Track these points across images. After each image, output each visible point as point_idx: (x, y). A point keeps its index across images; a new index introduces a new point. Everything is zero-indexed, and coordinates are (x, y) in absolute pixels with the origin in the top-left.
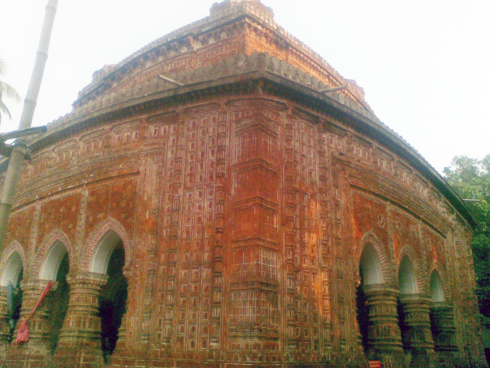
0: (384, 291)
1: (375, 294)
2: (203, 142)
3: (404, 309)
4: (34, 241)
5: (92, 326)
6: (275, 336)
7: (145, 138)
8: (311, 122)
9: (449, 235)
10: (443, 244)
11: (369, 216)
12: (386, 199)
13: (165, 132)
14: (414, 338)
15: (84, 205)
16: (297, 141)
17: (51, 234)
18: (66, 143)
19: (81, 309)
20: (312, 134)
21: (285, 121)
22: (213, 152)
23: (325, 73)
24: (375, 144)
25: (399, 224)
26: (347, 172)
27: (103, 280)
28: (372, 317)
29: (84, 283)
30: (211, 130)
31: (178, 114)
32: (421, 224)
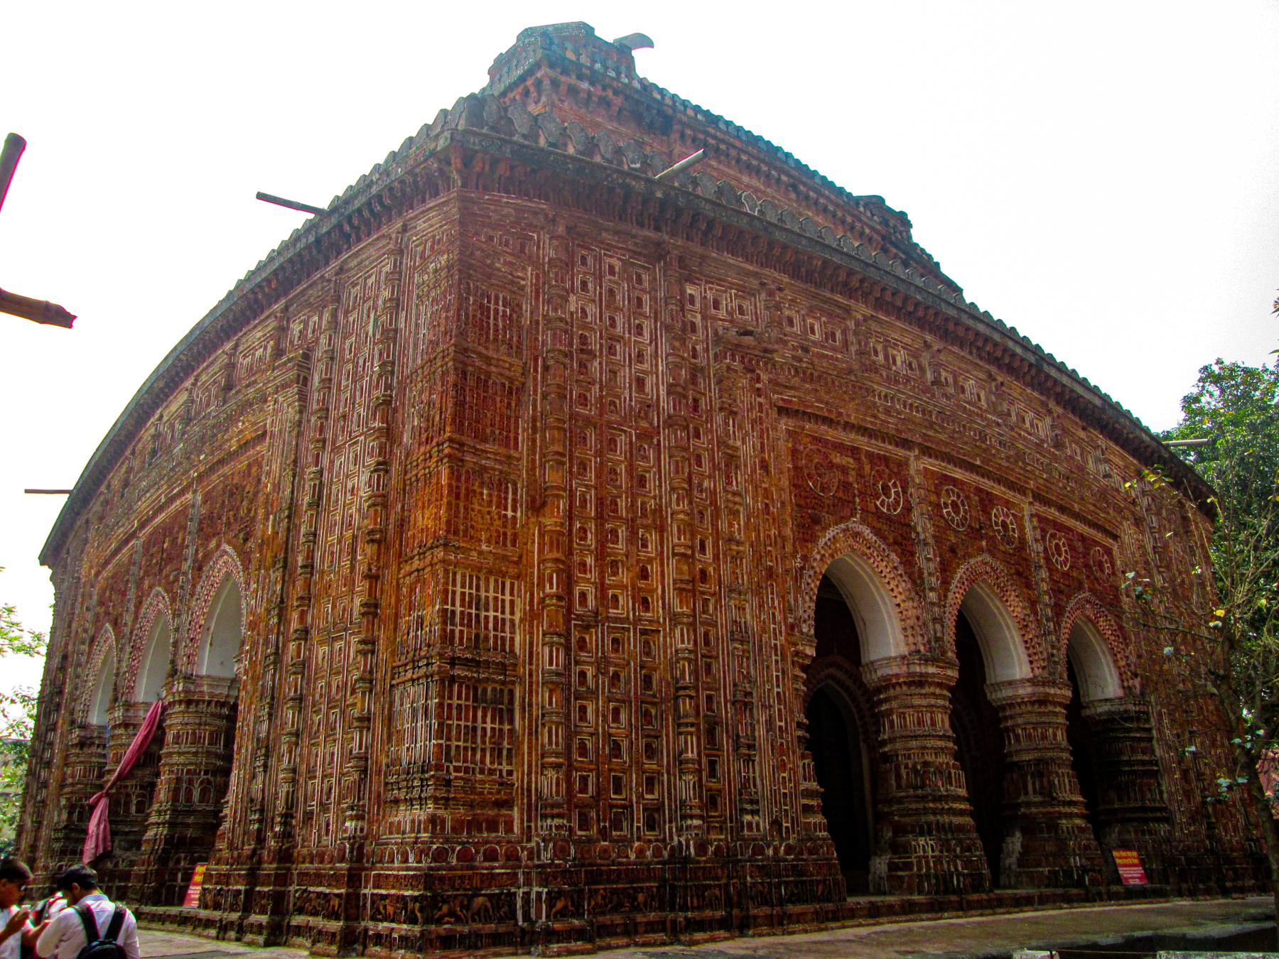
0: (909, 674)
1: (888, 683)
3: (999, 721)
6: (502, 796)
9: (1128, 532)
10: (1109, 552)
11: (846, 486)
12: (906, 444)
14: (1026, 793)
19: (182, 759)
23: (784, 178)
24: (862, 310)
25: (954, 505)
26: (764, 377)
28: (884, 743)
32: (1031, 503)
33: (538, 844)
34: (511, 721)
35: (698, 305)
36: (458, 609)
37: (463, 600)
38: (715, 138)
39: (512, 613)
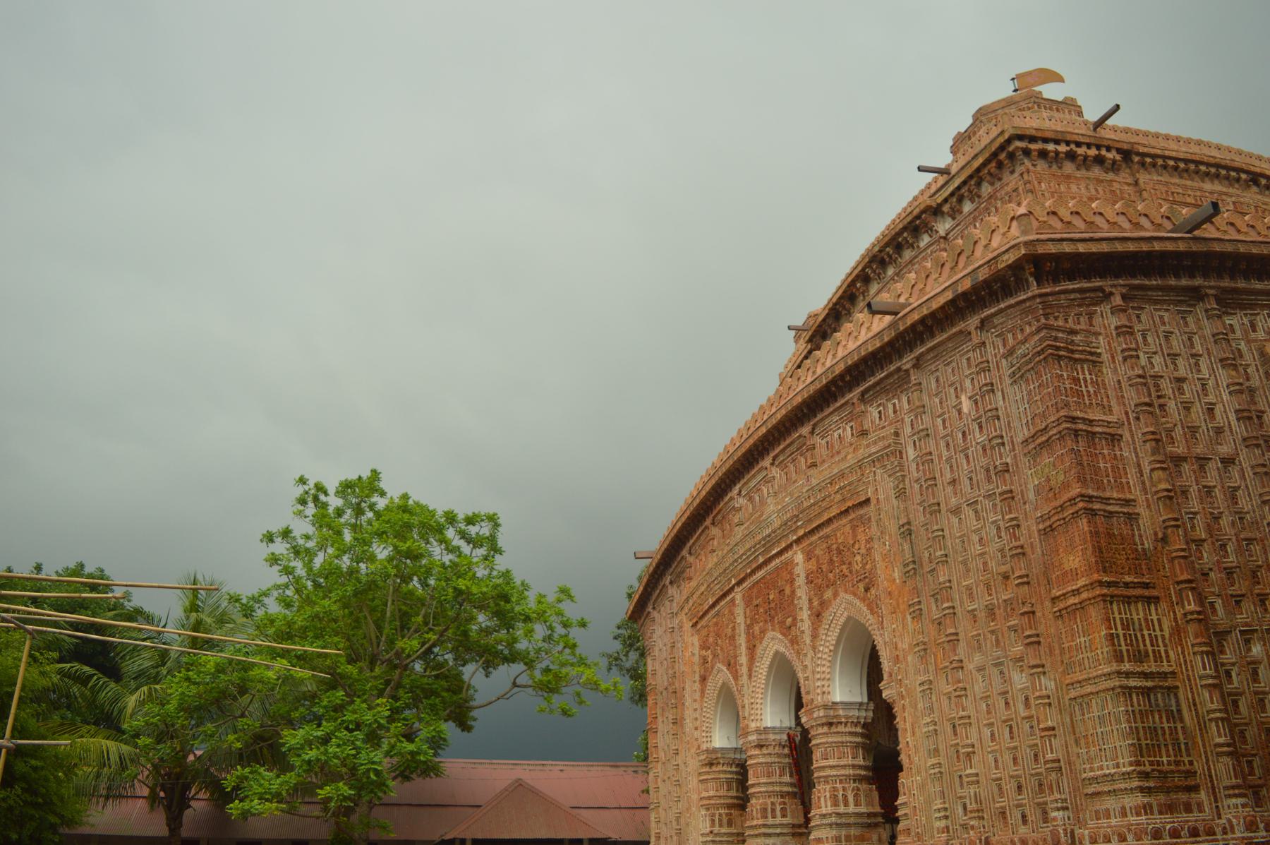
2: (960, 412)
4: (743, 660)
5: (861, 804)
7: (864, 433)
8: (1180, 302)
13: (895, 412)
15: (801, 581)
16: (1155, 353)
17: (765, 643)
18: (754, 476)
20: (1193, 327)
21: (1114, 321)
22: (981, 427)
23: (1244, 176)
27: (863, 714)
29: (831, 724)
30: (968, 383)
31: (907, 371)
33: (1229, 821)
34: (1182, 720)
35: (1239, 334)
36: (1121, 632)
37: (1122, 624)
38: (1171, 158)
39: (1161, 630)
